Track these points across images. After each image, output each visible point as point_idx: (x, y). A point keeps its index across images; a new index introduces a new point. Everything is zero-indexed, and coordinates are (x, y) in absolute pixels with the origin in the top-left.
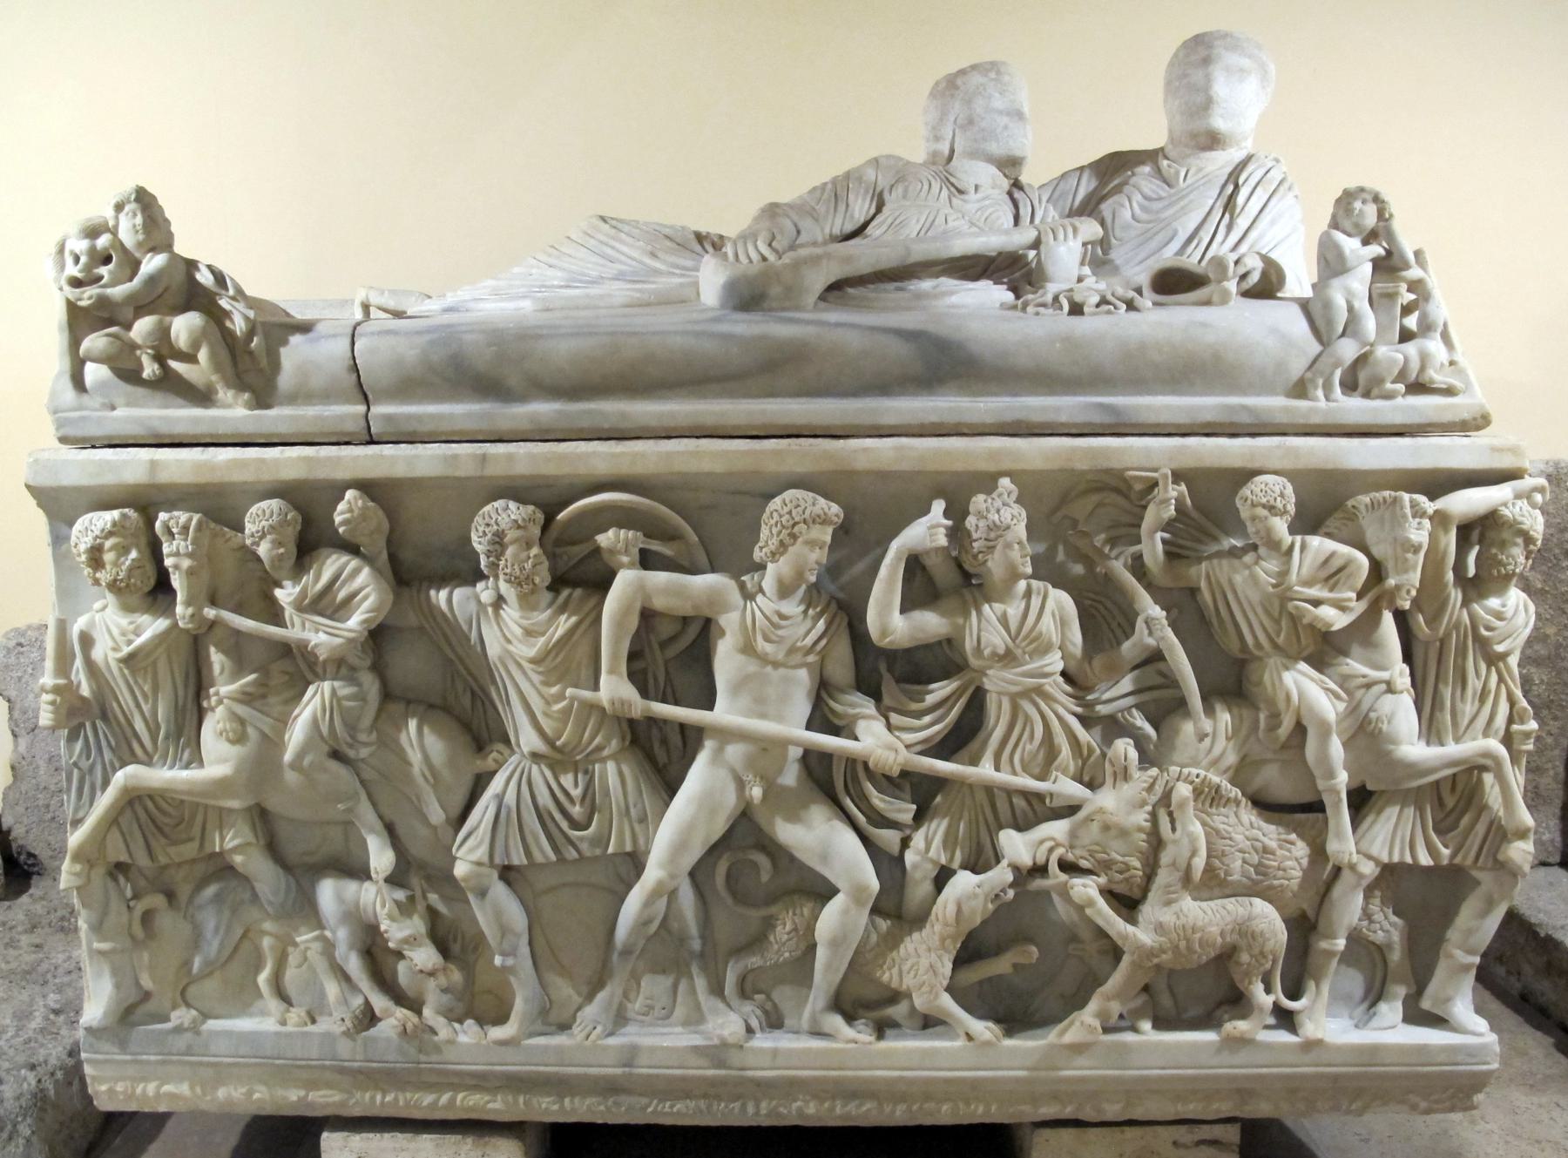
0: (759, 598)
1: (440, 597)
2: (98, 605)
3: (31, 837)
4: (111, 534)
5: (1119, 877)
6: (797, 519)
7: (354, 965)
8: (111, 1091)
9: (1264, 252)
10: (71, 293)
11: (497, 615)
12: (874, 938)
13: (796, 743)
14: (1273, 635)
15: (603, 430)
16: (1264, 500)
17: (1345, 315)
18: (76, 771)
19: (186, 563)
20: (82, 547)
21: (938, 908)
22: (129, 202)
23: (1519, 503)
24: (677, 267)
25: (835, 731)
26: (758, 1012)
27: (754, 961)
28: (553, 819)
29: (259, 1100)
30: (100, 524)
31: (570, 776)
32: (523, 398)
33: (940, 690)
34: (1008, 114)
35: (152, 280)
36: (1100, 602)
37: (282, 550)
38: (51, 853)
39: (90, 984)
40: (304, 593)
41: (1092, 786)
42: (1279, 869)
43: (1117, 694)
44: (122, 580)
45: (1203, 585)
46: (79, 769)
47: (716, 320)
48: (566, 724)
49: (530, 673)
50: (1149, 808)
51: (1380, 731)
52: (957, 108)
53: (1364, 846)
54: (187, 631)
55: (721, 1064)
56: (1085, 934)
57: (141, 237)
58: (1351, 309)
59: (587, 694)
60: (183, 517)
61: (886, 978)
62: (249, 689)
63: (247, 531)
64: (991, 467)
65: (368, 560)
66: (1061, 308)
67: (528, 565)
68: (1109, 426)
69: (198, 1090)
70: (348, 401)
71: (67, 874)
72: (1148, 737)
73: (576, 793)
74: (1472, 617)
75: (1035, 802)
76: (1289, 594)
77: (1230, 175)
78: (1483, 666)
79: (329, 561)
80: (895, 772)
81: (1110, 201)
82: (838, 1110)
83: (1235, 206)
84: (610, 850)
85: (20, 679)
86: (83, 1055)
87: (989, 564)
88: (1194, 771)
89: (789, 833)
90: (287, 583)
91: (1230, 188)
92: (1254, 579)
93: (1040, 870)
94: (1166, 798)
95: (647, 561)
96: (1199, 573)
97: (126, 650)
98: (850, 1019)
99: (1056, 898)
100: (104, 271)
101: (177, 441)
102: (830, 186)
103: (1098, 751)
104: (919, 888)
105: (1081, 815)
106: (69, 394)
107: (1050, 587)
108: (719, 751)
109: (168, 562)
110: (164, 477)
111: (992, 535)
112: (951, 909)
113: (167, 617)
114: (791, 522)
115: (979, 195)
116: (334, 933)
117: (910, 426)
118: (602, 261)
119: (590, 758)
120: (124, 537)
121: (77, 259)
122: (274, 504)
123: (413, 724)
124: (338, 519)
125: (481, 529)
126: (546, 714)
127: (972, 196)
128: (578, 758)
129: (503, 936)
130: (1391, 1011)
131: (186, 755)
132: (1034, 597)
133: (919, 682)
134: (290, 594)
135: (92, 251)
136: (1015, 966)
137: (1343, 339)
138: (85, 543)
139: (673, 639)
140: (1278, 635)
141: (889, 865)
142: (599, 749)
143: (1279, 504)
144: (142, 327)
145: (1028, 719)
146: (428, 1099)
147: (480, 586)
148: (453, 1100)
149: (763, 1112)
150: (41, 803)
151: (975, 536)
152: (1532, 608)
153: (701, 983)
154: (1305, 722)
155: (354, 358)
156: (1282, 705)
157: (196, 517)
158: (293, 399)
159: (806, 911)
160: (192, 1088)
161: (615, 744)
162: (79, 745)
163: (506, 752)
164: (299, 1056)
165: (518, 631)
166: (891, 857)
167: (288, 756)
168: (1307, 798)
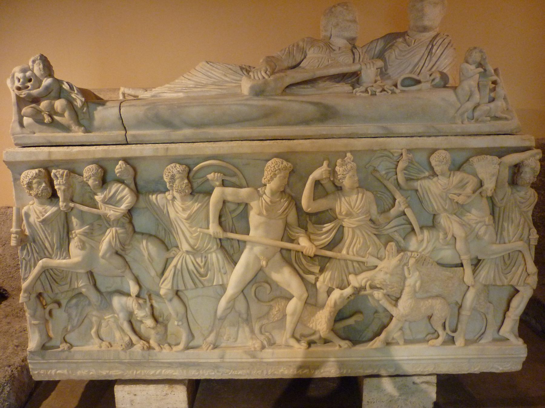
0: (264, 196)
1: (153, 198)
2: (31, 203)
3: (5, 283)
4: (35, 178)
6: (277, 169)
7: (126, 326)
8: (39, 373)
9: (441, 70)
11: (173, 204)
18: (24, 261)
19: (63, 188)
20: (25, 183)
21: (328, 302)
22: (37, 60)
24: (234, 80)
25: (292, 241)
27: (265, 321)
28: (193, 272)
29: (92, 375)
30: (31, 174)
31: (200, 259)
32: (179, 128)
33: (328, 226)
35: (47, 88)
36: (382, 195)
37: (97, 182)
38: (12, 289)
39: (31, 336)
40: (105, 197)
44: (39, 194)
45: (419, 188)
46: (25, 260)
47: (247, 100)
48: (198, 241)
49: (185, 223)
50: (401, 267)
54: (64, 211)
55: (254, 357)
56: (380, 310)
57: (42, 72)
58: (471, 91)
59: (206, 231)
60: (61, 171)
61: (311, 326)
62: (87, 231)
63: (84, 176)
64: (344, 149)
65: (127, 185)
66: (368, 93)
67: (184, 186)
69: (70, 372)
70: (119, 130)
71: (22, 298)
73: (202, 264)
75: (361, 264)
77: (431, 41)
79: (114, 186)
80: (312, 255)
81: (388, 52)
84: (215, 284)
86: (28, 361)
87: (344, 183)
88: (416, 254)
89: (276, 277)
90: (99, 194)
91: (430, 46)
94: (406, 264)
95: (224, 184)
96: (417, 184)
97: (42, 218)
98: (298, 341)
99: (369, 298)
100: (29, 84)
102: (287, 49)
104: (322, 295)
105: (377, 269)
106: (18, 129)
107: (365, 191)
108: (252, 249)
109: (56, 187)
110: (53, 157)
111: (345, 173)
112: (333, 302)
113: (56, 207)
114: (275, 170)
116: (118, 315)
118: (207, 78)
119: (207, 252)
120: (40, 179)
121: (19, 80)
122: (94, 166)
123: (144, 242)
124: (116, 171)
125: (167, 174)
126: (191, 238)
128: (202, 252)
131: (64, 254)
133: (320, 224)
134: (100, 198)
135: (25, 77)
136: (355, 321)
138: (26, 181)
139: (234, 210)
140: (446, 206)
142: (210, 249)
144: (44, 104)
145: (358, 235)
146: (152, 372)
147: (167, 193)
148: (161, 372)
149: (270, 373)
150: (8, 271)
151: (339, 173)
152: (536, 195)
153: (247, 329)
154: (455, 236)
155: (121, 115)
156: (448, 231)
157: (66, 171)
158: (99, 129)
159: (283, 304)
160: (68, 371)
161: (215, 247)
162: (25, 252)
163: (178, 251)
164: (107, 359)
165: (181, 209)
166: (312, 284)
167: (101, 254)
168: (458, 262)
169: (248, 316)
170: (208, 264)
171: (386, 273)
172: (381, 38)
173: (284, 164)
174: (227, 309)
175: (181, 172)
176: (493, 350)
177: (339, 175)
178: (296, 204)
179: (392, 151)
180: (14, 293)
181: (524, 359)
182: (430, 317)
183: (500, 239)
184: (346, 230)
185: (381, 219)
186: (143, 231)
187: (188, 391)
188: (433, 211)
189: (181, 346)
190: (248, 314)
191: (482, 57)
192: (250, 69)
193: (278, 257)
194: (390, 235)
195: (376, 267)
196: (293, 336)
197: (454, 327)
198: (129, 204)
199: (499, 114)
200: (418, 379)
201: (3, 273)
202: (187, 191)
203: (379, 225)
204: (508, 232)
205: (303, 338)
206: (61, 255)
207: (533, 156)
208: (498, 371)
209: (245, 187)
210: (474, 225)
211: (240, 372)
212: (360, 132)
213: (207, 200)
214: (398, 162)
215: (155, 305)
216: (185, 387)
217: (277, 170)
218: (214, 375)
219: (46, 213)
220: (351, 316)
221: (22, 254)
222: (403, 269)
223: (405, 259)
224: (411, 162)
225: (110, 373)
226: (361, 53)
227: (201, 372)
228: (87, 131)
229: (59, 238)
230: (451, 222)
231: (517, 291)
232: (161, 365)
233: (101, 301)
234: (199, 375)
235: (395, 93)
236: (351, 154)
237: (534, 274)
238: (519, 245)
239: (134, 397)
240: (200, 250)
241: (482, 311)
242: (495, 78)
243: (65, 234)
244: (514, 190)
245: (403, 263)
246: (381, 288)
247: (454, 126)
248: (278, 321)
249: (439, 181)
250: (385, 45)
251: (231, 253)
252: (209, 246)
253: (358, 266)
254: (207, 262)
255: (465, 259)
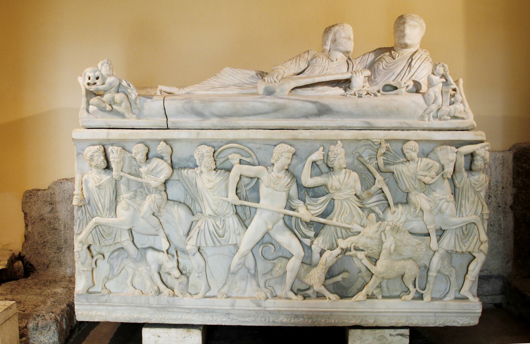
1: (185, 172)
3: (31, 258)
5: (370, 252)
6: (283, 151)
7: (156, 277)
8: (82, 314)
10: (87, 87)
12: (303, 270)
13: (282, 213)
14: (414, 185)
15: (231, 127)
16: (409, 148)
17: (434, 97)
18: (78, 219)
19: (117, 160)
20: (88, 156)
23: (482, 149)
24: (251, 83)
26: (270, 291)
27: (269, 277)
29: (125, 317)
31: (219, 222)
34: (346, 38)
38: (37, 264)
40: (148, 170)
41: (363, 226)
42: (416, 251)
43: (371, 202)
45: (395, 171)
46: (80, 219)
50: (379, 233)
51: (444, 213)
52: (331, 36)
53: (441, 245)
55: (259, 306)
56: (363, 269)
58: (435, 96)
60: (116, 148)
61: (306, 281)
63: (133, 152)
64: (335, 138)
65: (166, 161)
66: (356, 95)
68: (368, 127)
72: (380, 214)
73: (221, 226)
74: (470, 181)
75: (348, 231)
76: (417, 173)
77: (411, 56)
78: (473, 194)
82: (292, 321)
83: (411, 65)
84: (229, 244)
85: (30, 206)
87: (334, 164)
90: (143, 167)
91: (410, 60)
92: (409, 170)
93: (348, 250)
94: (384, 231)
95: (241, 162)
96: (392, 168)
97: (98, 184)
98: (296, 294)
99: (355, 259)
100: (97, 81)
101: (114, 127)
103: (365, 217)
104: (316, 256)
105: (360, 234)
107: (351, 171)
110: (111, 137)
111: (335, 156)
115: (337, 62)
116: (150, 267)
117: (313, 127)
119: (225, 216)
121: (89, 79)
124: (158, 149)
125: (197, 153)
127: (335, 62)
129: (199, 267)
130: (452, 295)
131: (112, 215)
132: (347, 174)
136: (342, 278)
137: (433, 104)
139: (248, 185)
140: (415, 186)
141: (307, 249)
142: (228, 214)
143: (414, 149)
145: (345, 206)
147: (196, 169)
149: (271, 321)
150: (35, 247)
151: (331, 157)
153: (254, 283)
156: (417, 205)
159: (284, 262)
161: (232, 212)
162: (80, 212)
167: (142, 214)
168: (426, 232)
169: (255, 272)
170: (226, 226)
171: (367, 237)
172: (372, 52)
173: (288, 148)
174: (239, 265)
175: (209, 151)
176: (455, 306)
177: (331, 158)
178: (297, 181)
179: (374, 140)
180: (39, 267)
181: (480, 315)
182: (402, 276)
183: (460, 214)
184: (336, 202)
185: (364, 195)
186: (175, 199)
187: (202, 335)
188: (406, 190)
189: (200, 295)
190: (255, 270)
191: (444, 70)
192: (263, 74)
193: (281, 222)
194: (372, 208)
195: (360, 232)
196: (292, 290)
197: (423, 286)
198: (167, 175)
199: (457, 114)
200: (394, 331)
201: (30, 249)
202: (212, 167)
203: (363, 200)
204: (465, 208)
205: (299, 292)
206: (110, 215)
207: (484, 147)
208: (459, 325)
209: (257, 166)
210: (438, 202)
211: (247, 319)
212: (348, 125)
213: (227, 174)
214: (378, 149)
215: (180, 260)
216: (200, 331)
217: (283, 152)
218: (225, 321)
219: (101, 180)
220: (339, 274)
221: (77, 214)
222: (381, 235)
223: (383, 227)
224: (388, 150)
225: (140, 316)
226: (354, 64)
227: (215, 318)
228: (139, 117)
229: (109, 201)
230: (420, 199)
231: (475, 257)
232: (182, 310)
233: (138, 255)
234: (212, 320)
235: (377, 96)
236: (341, 142)
237: (485, 242)
238: (473, 218)
239: (158, 339)
240: (219, 215)
241: (446, 273)
242: (454, 86)
243: (114, 198)
244: (470, 175)
245: (381, 230)
246: (363, 250)
247: (422, 122)
248: (279, 276)
249: (410, 165)
250: (375, 58)
251: (244, 219)
252: (228, 211)
253: (345, 232)
254: (225, 225)
255: (432, 229)
